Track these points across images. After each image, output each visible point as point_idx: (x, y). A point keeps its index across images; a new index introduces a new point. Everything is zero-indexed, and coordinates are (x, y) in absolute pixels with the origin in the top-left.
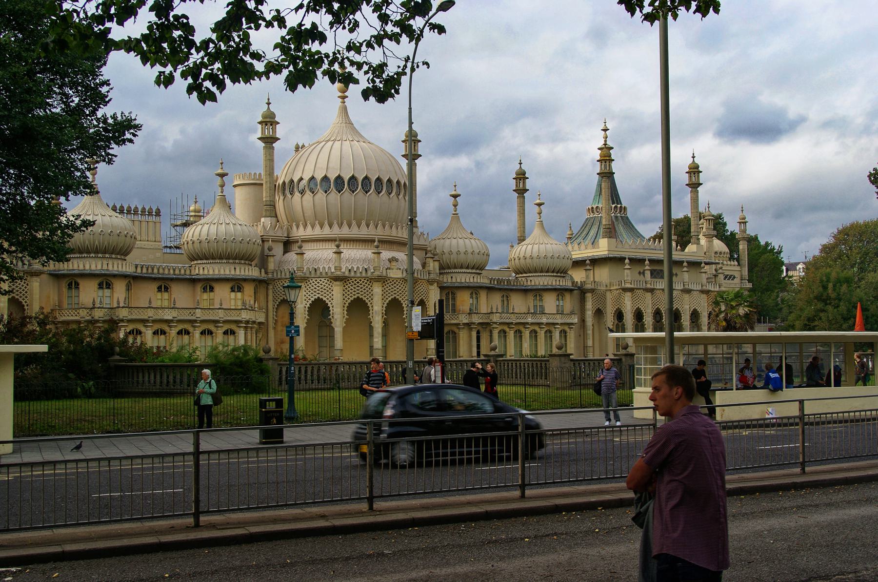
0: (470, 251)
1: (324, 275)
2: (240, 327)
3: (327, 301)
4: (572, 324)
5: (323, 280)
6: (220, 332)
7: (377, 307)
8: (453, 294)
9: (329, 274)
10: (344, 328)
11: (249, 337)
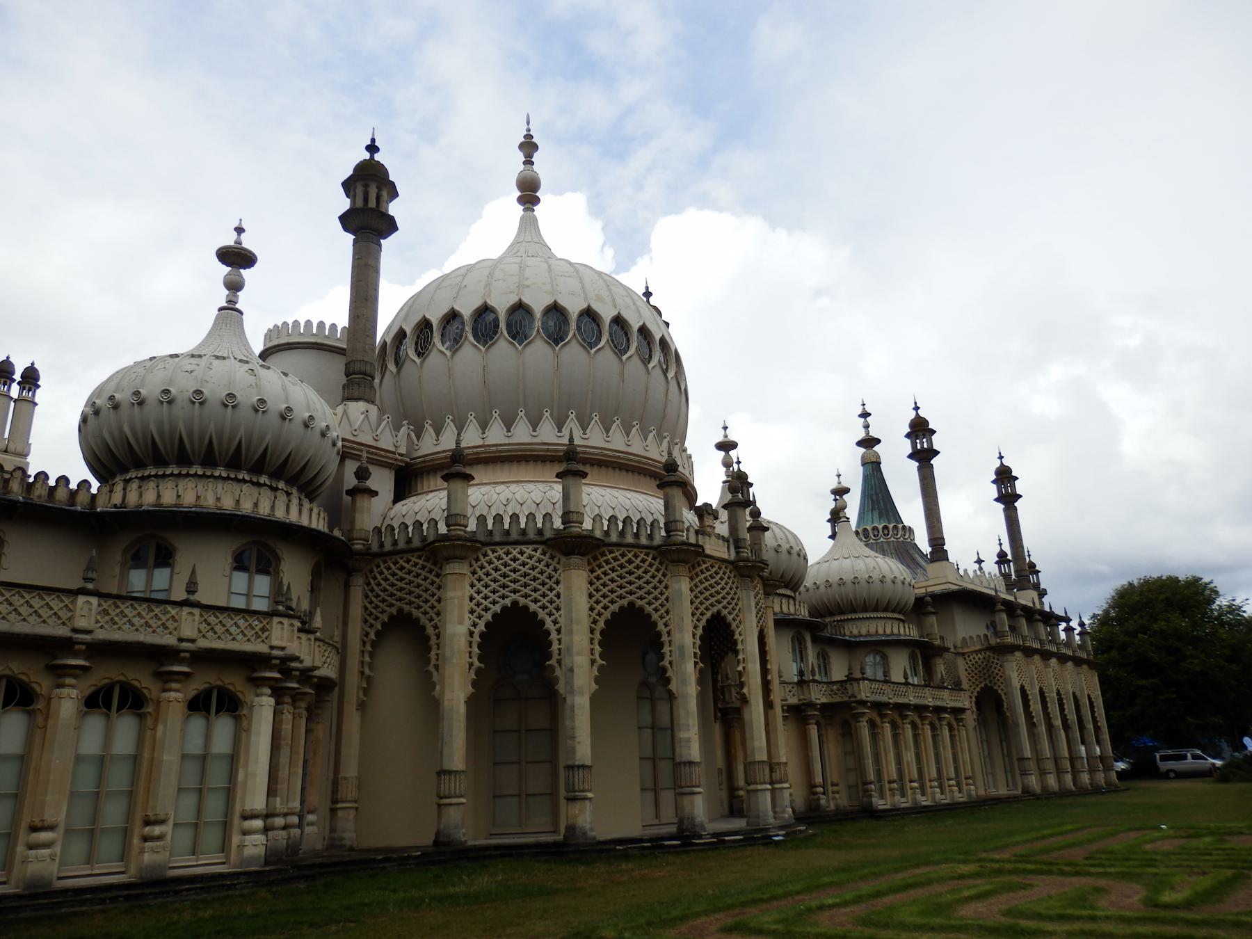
0: (785, 547)
1: (532, 535)
2: (257, 682)
3: (542, 614)
4: (963, 710)
5: (528, 550)
6: (177, 697)
7: (683, 636)
9: (548, 534)
10: (594, 699)
11: (287, 727)
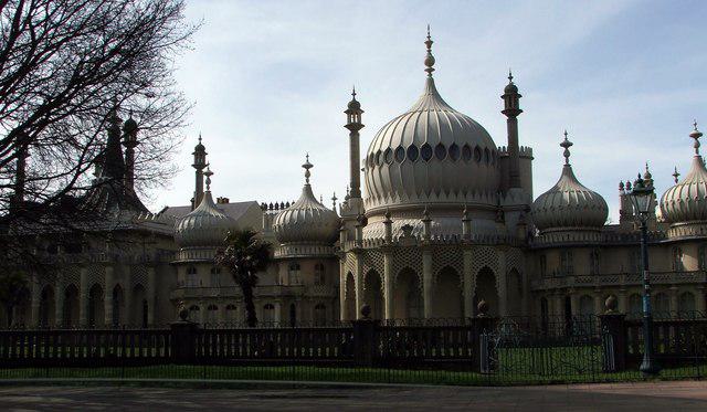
8: (545, 257)
